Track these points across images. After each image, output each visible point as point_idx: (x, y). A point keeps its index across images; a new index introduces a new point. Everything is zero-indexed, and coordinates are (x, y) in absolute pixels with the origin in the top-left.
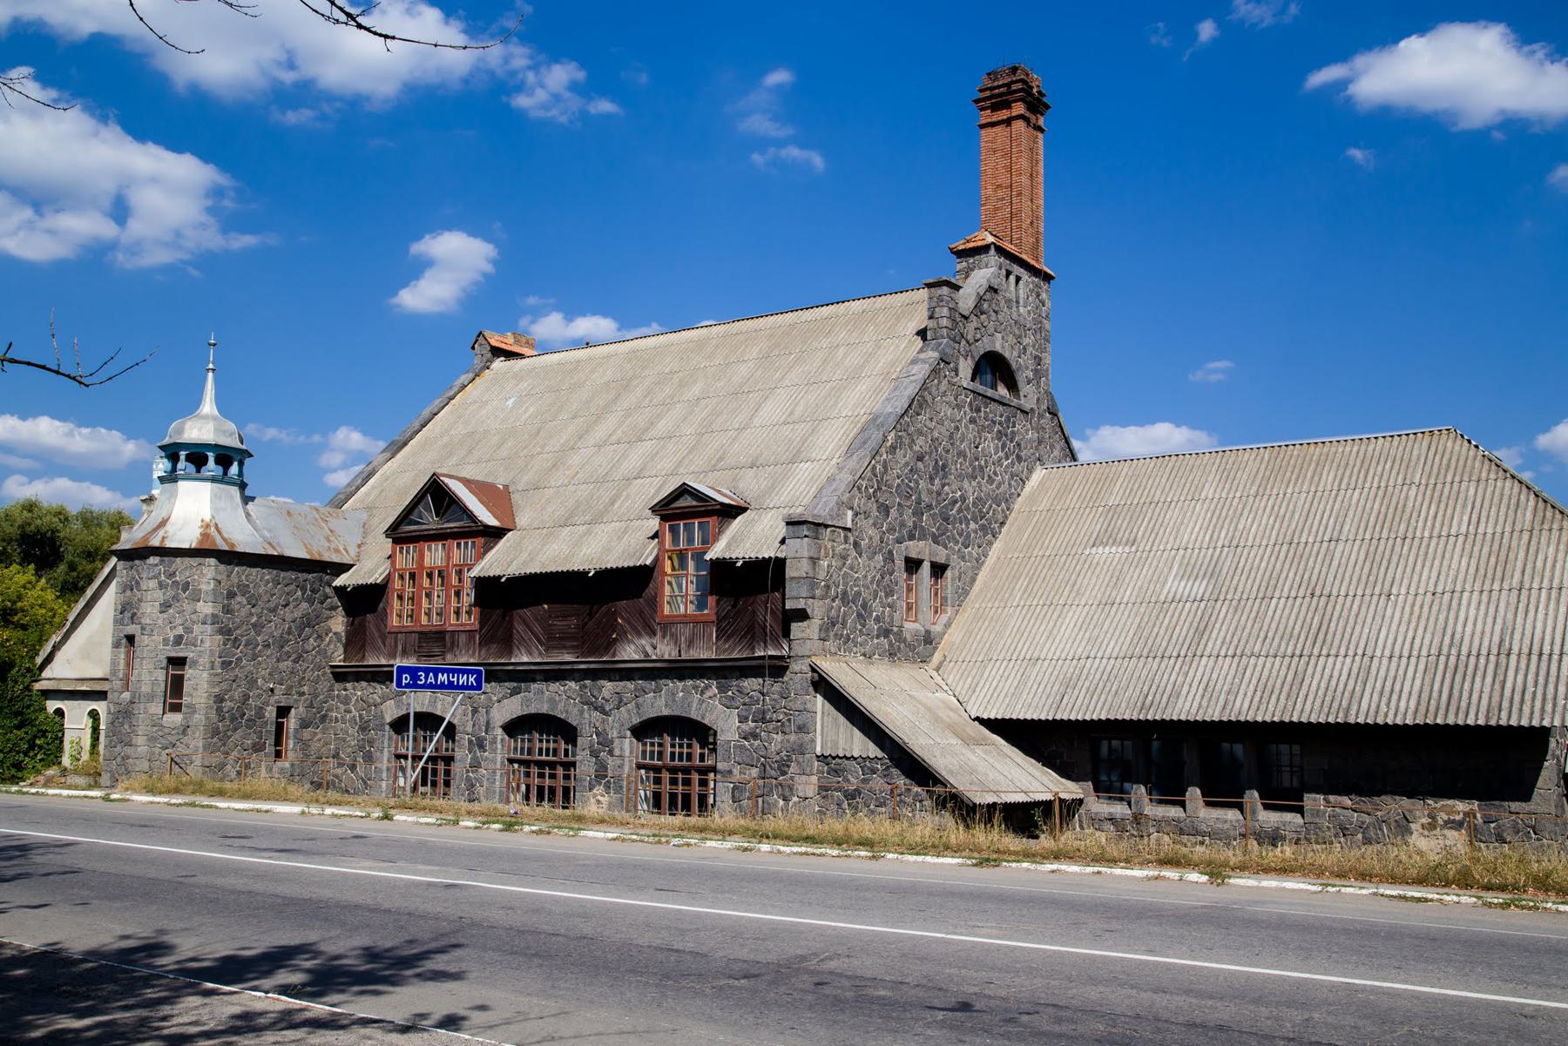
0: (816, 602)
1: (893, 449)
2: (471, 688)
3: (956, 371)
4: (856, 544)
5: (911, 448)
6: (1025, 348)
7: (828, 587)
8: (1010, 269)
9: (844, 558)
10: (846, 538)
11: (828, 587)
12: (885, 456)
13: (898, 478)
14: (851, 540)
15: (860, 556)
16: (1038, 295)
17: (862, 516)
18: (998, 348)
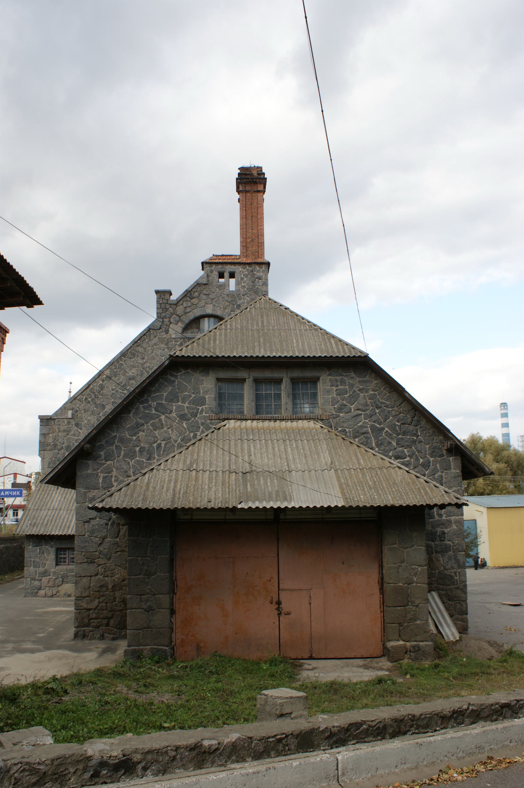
0: (46, 452)
1: (109, 378)
2: (18, 496)
3: (167, 332)
4: (77, 425)
5: (124, 375)
6: (239, 306)
7: (55, 445)
8: (222, 270)
9: (67, 431)
10: (69, 423)
11: (55, 445)
12: (101, 382)
13: (113, 390)
14: (74, 423)
15: (81, 429)
16: (253, 275)
17: (83, 411)
18: (209, 310)
